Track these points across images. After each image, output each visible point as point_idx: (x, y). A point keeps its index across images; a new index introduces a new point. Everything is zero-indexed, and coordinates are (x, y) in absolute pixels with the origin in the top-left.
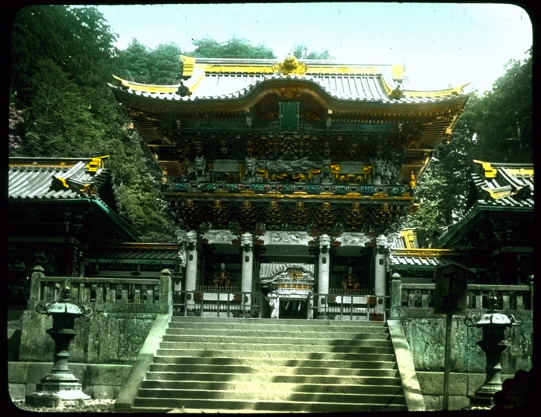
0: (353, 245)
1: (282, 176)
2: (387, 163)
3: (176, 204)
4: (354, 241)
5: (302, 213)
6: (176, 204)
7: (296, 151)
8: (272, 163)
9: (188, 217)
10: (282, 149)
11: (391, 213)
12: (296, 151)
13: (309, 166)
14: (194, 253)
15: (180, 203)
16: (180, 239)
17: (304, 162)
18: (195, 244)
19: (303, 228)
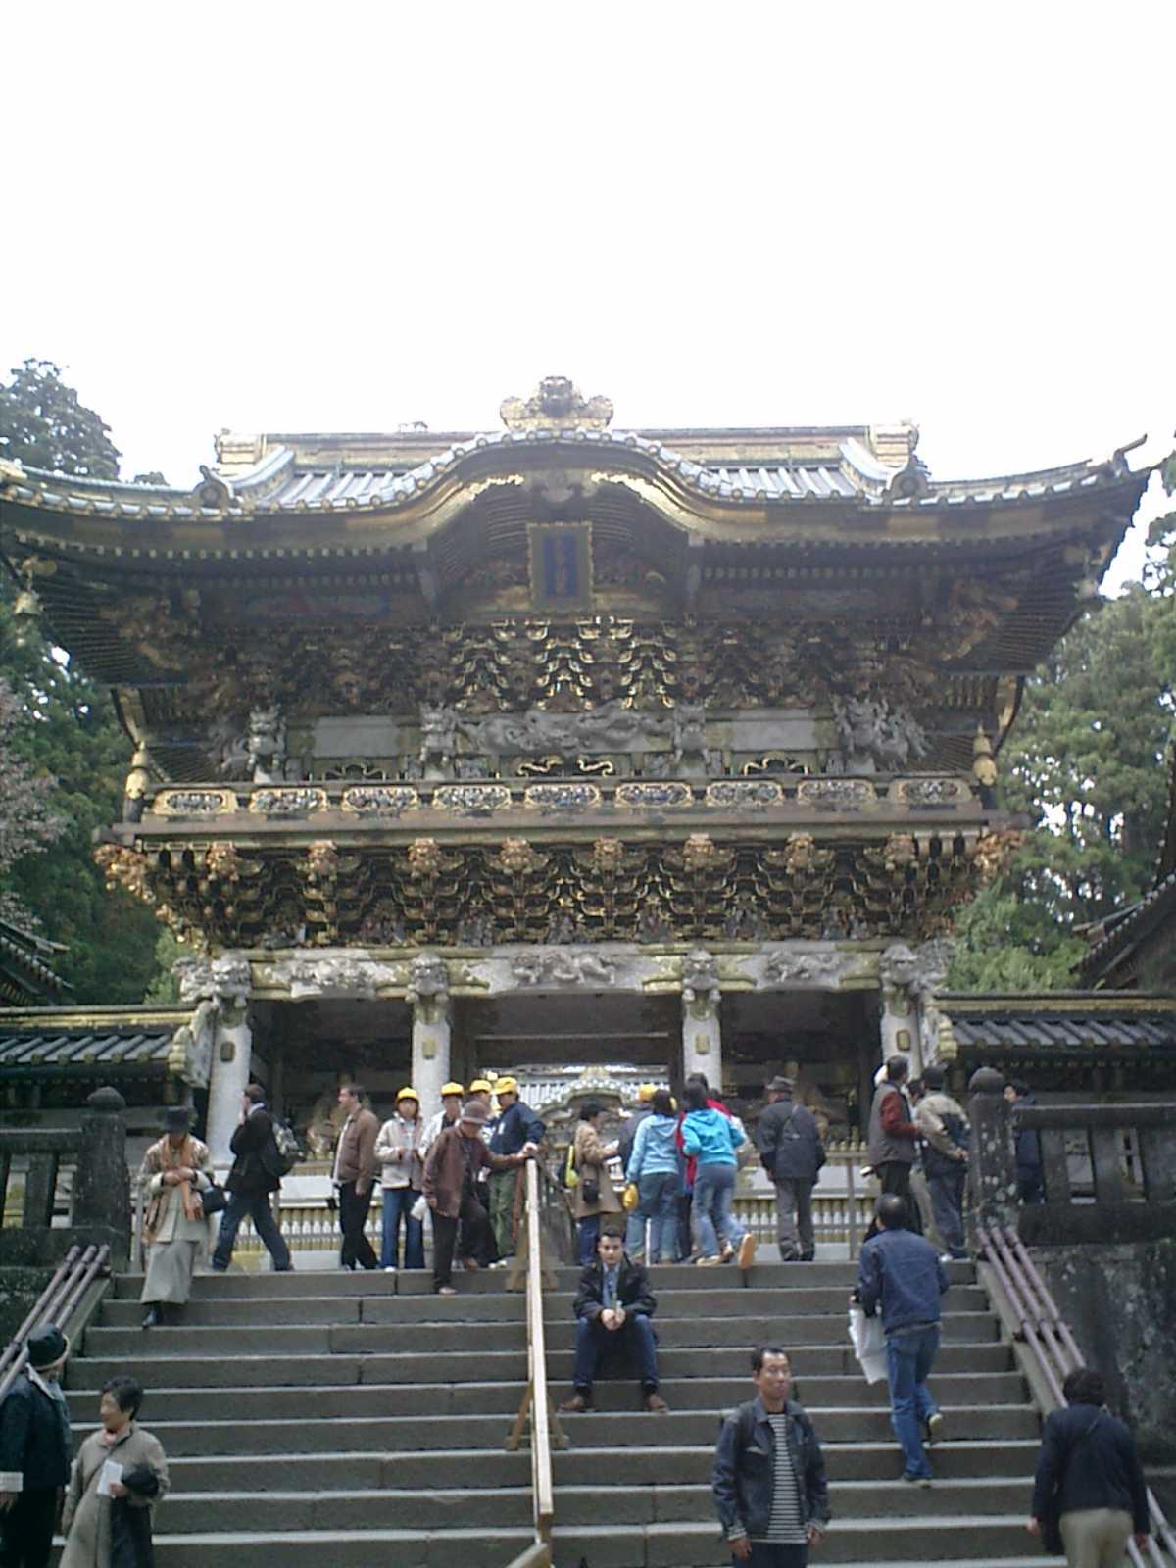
0: (799, 984)
1: (544, 766)
2: (891, 712)
3: (176, 860)
4: (802, 971)
5: (618, 878)
6: (176, 860)
7: (588, 682)
8: (507, 722)
9: (220, 908)
10: (542, 674)
11: (922, 868)
12: (588, 682)
13: (629, 728)
14: (238, 1036)
15: (188, 856)
16: (190, 989)
17: (614, 716)
18: (240, 1003)
19: (622, 931)
